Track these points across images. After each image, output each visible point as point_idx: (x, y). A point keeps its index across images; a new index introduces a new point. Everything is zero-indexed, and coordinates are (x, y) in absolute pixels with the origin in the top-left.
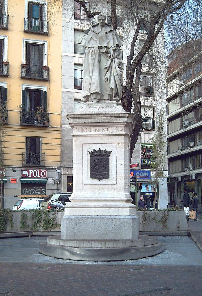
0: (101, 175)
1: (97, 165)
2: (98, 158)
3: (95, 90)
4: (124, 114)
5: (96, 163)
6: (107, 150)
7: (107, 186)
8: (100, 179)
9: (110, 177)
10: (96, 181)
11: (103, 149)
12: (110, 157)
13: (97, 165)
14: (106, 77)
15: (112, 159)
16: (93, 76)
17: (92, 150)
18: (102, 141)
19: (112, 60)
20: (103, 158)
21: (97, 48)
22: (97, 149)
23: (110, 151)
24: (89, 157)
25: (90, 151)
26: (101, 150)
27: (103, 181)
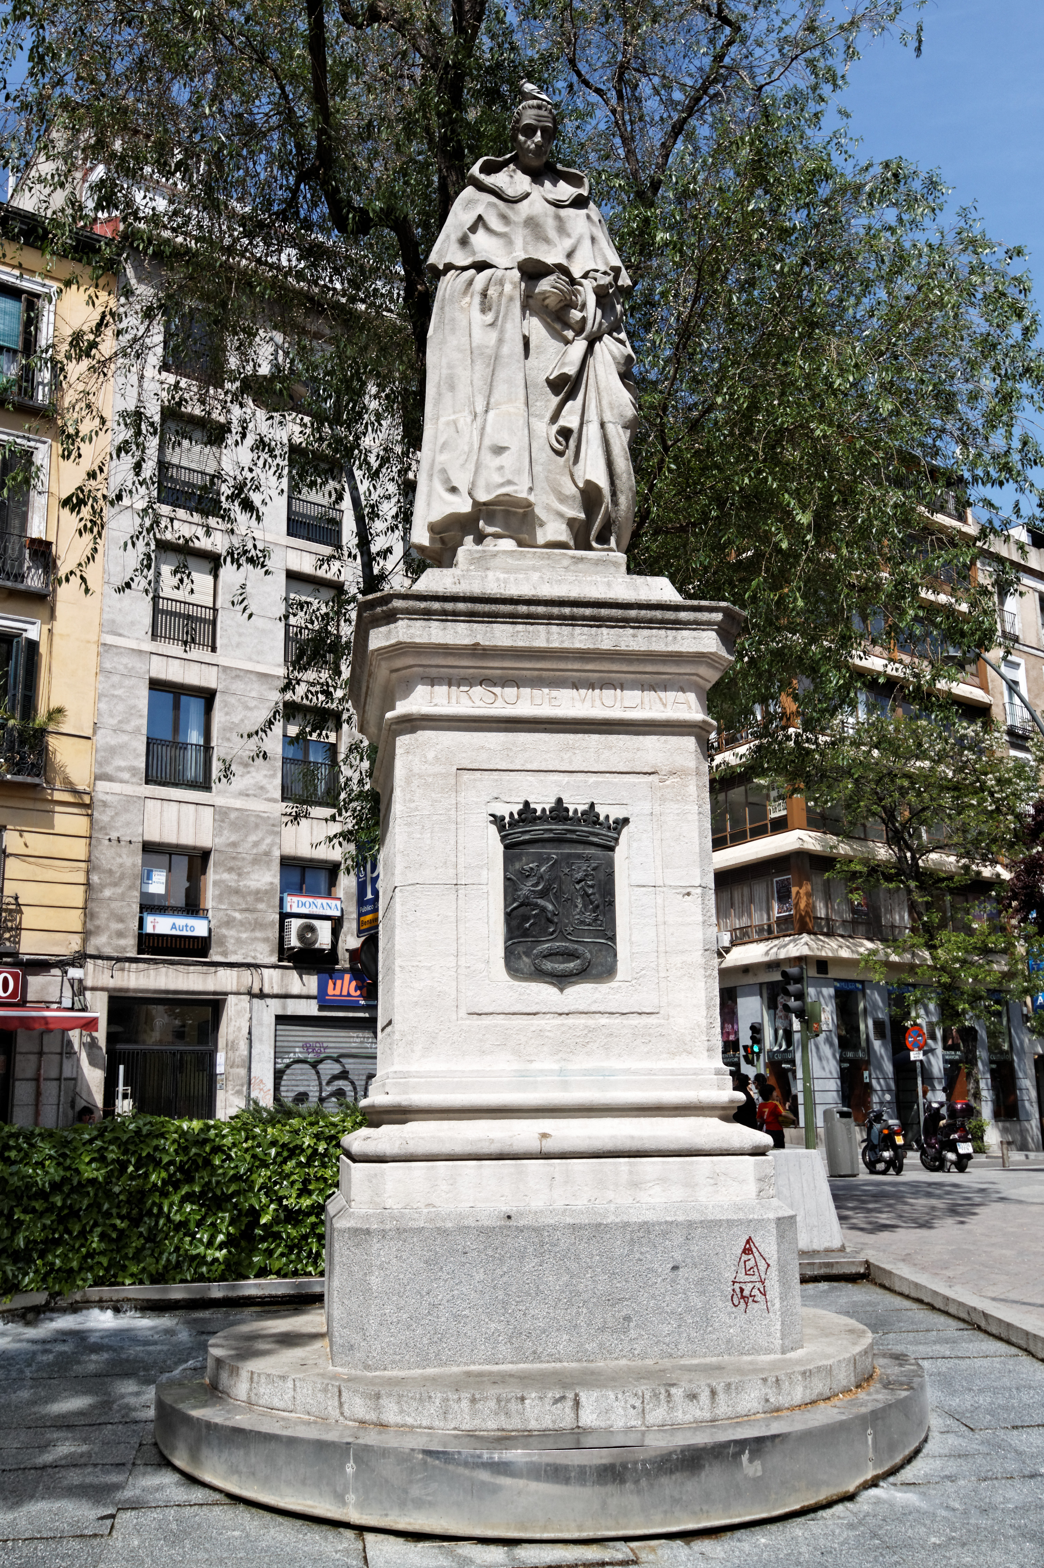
0: (572, 955)
1: (543, 894)
2: (554, 852)
3: (509, 482)
4: (677, 608)
5: (537, 884)
6: (602, 811)
7: (604, 1020)
8: (561, 980)
9: (621, 966)
10: (542, 993)
11: (575, 804)
12: (620, 855)
13: (543, 894)
14: (562, 422)
15: (629, 863)
16: (491, 414)
17: (516, 809)
18: (569, 754)
19: (592, 342)
20: (579, 856)
21: (516, 274)
22: (542, 803)
23: (616, 813)
24: (494, 846)
25: (503, 810)
26: (567, 810)
27: (581, 994)
